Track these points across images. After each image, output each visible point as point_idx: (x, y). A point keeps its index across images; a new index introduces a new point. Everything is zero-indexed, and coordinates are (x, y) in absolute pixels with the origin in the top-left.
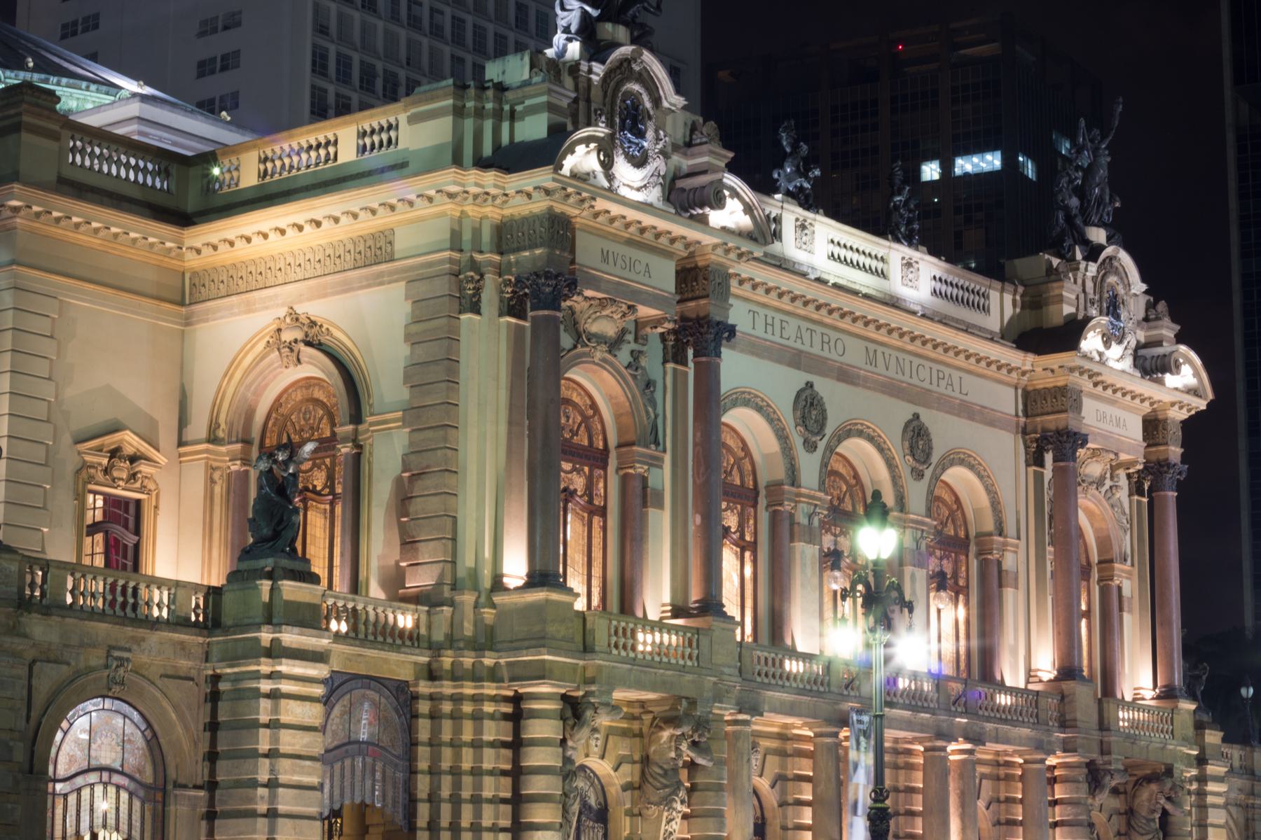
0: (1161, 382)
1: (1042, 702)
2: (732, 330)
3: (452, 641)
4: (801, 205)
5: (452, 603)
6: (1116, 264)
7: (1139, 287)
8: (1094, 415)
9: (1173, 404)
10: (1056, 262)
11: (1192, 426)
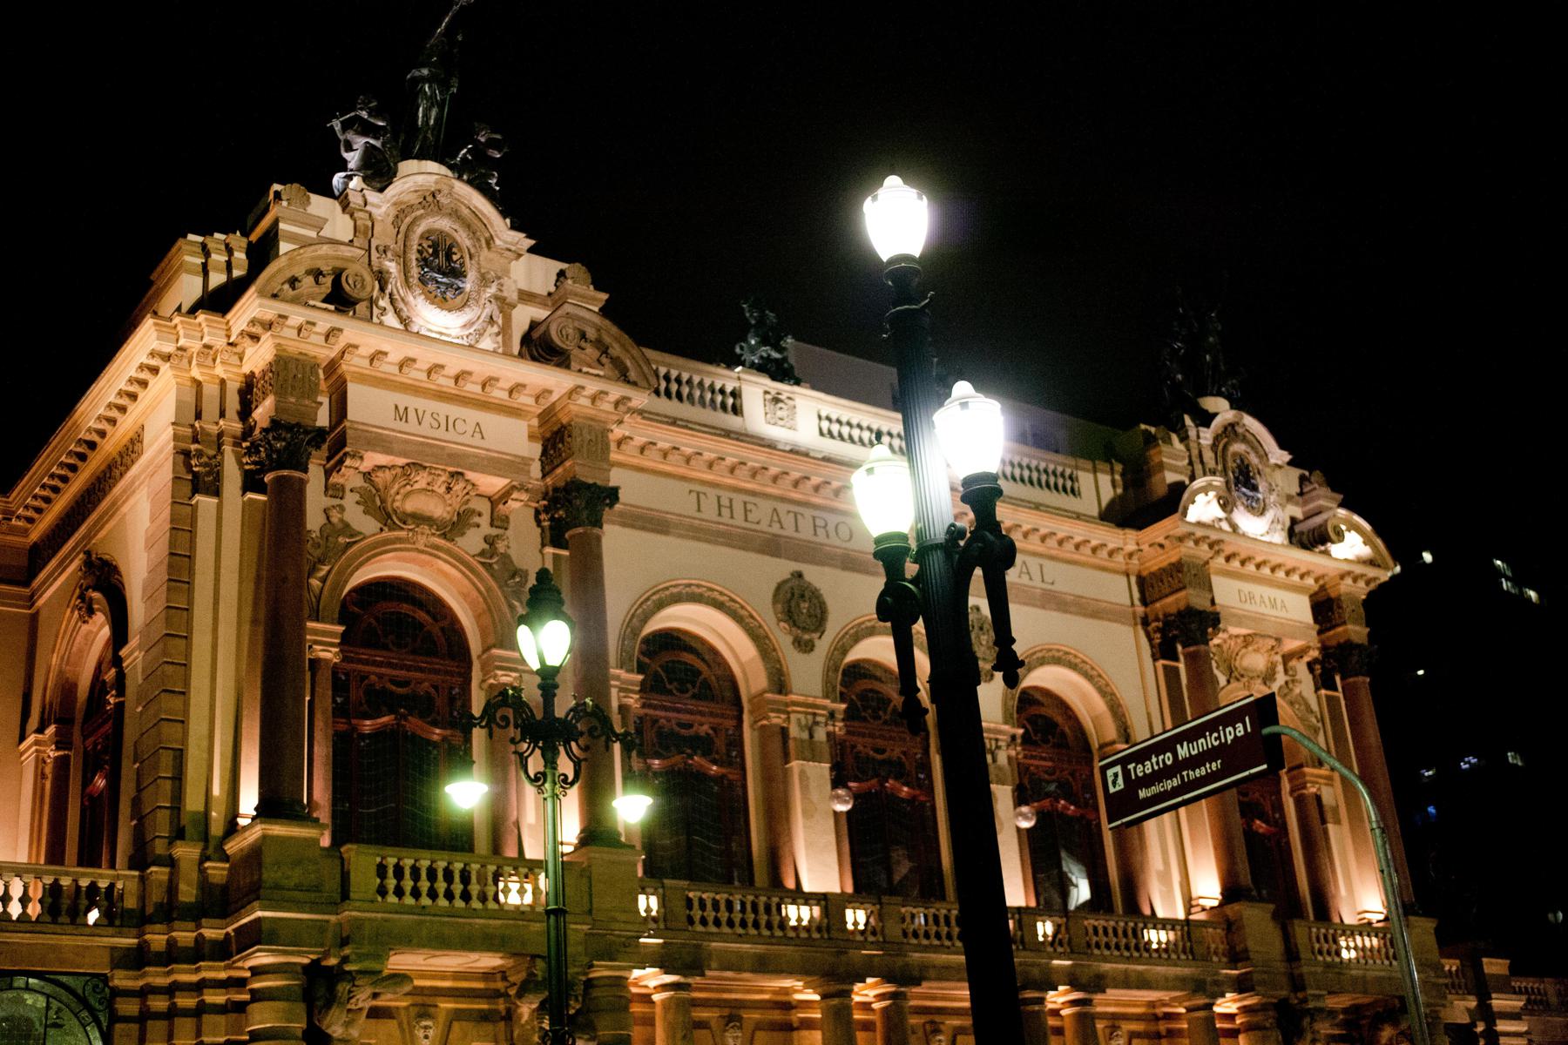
0: (1327, 553)
1: (1196, 934)
2: (612, 495)
3: (170, 912)
4: (774, 378)
5: (171, 862)
6: (1240, 430)
7: (1279, 456)
8: (1227, 592)
9: (1342, 577)
10: (1153, 430)
11: (1379, 602)
